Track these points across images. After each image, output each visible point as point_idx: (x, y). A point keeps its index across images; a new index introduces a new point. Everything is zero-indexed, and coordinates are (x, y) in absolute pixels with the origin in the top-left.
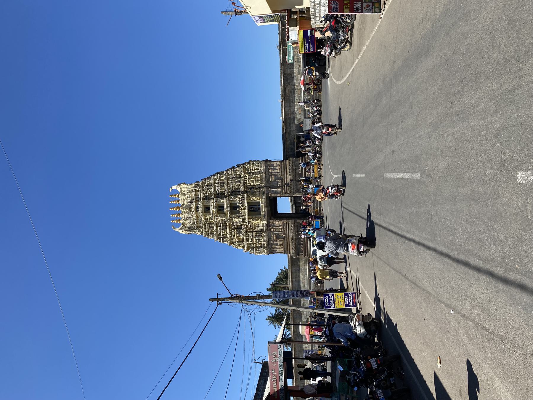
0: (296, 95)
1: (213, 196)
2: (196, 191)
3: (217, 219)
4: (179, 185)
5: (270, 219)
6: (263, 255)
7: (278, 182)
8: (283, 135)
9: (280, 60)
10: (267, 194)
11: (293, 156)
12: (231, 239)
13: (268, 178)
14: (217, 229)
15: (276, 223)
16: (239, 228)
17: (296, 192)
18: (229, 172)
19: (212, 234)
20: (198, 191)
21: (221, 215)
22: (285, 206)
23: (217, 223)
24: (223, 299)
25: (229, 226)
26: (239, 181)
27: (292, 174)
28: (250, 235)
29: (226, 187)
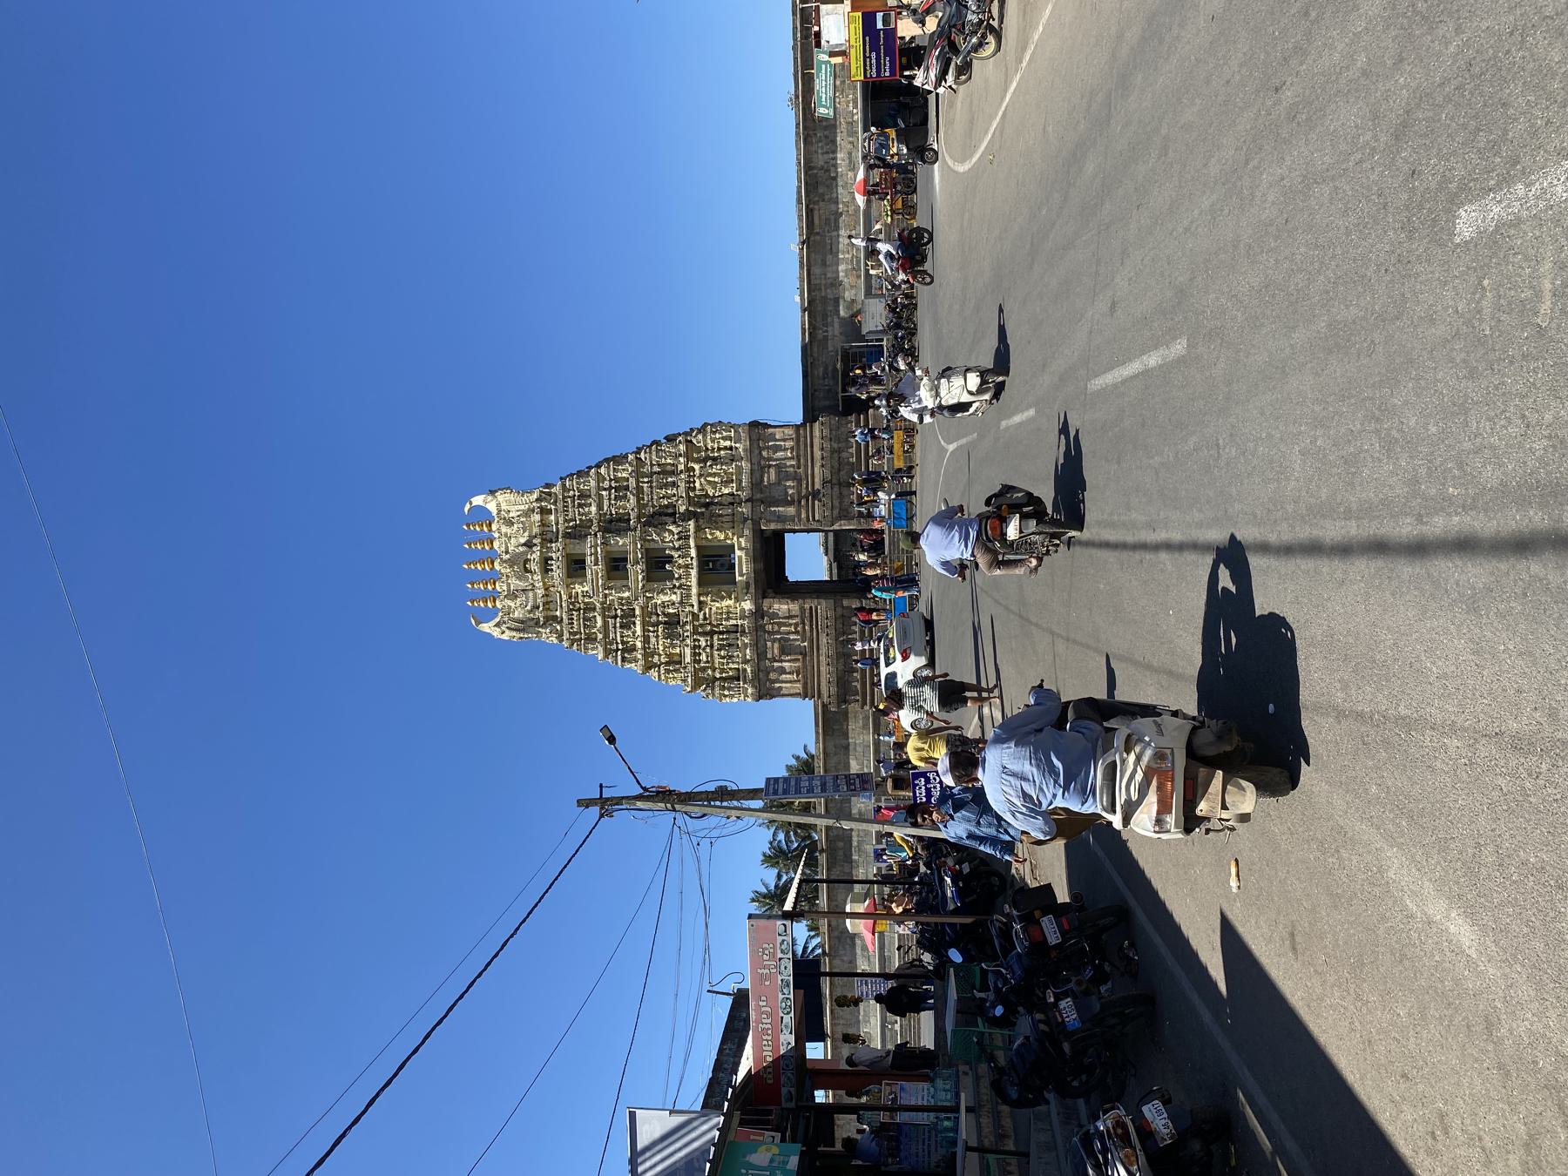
0: (842, 232)
1: (595, 528)
2: (544, 512)
3: (606, 596)
4: (492, 492)
5: (764, 597)
6: (741, 700)
7: (786, 488)
8: (804, 349)
9: (798, 125)
10: (756, 523)
11: (832, 410)
12: (648, 654)
13: (757, 475)
14: (605, 624)
15: (781, 607)
16: (672, 623)
17: (840, 518)
18: (642, 456)
19: (591, 639)
20: (550, 512)
21: (619, 583)
22: (807, 558)
23: (606, 609)
24: (619, 800)
25: (643, 616)
26: (674, 484)
27: (827, 462)
29: (633, 500)
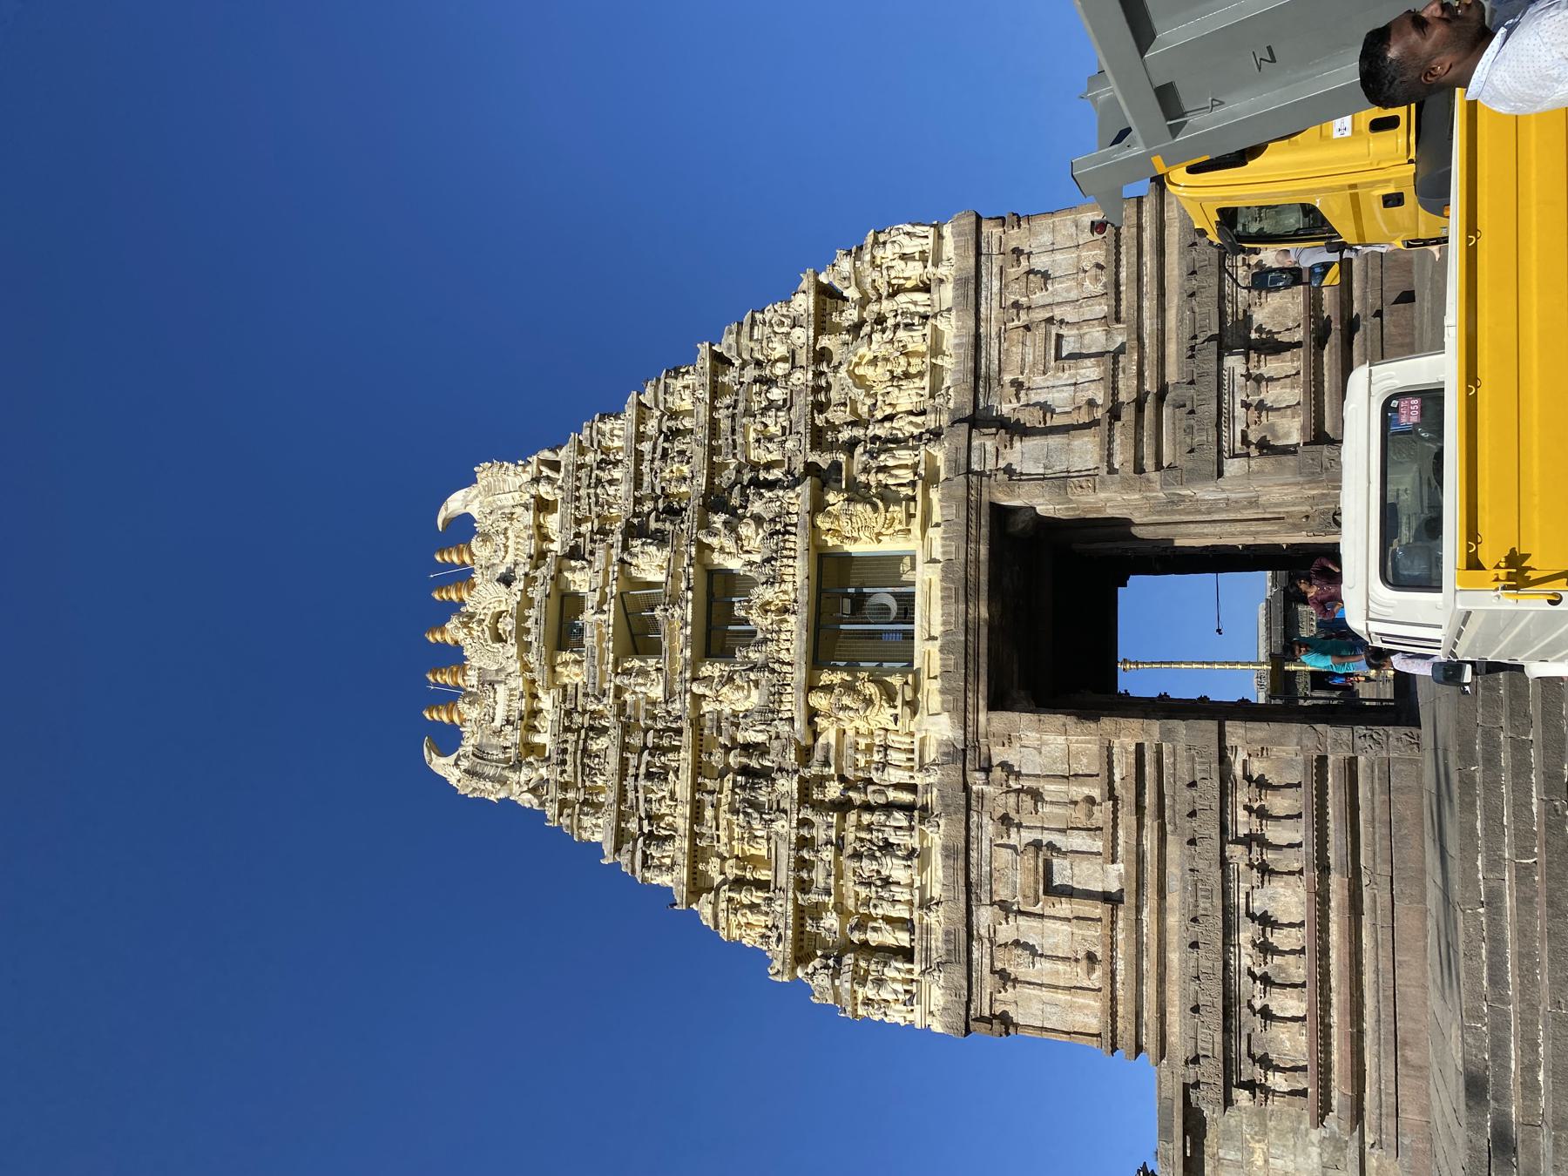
14: (624, 762)
28: (820, 834)
